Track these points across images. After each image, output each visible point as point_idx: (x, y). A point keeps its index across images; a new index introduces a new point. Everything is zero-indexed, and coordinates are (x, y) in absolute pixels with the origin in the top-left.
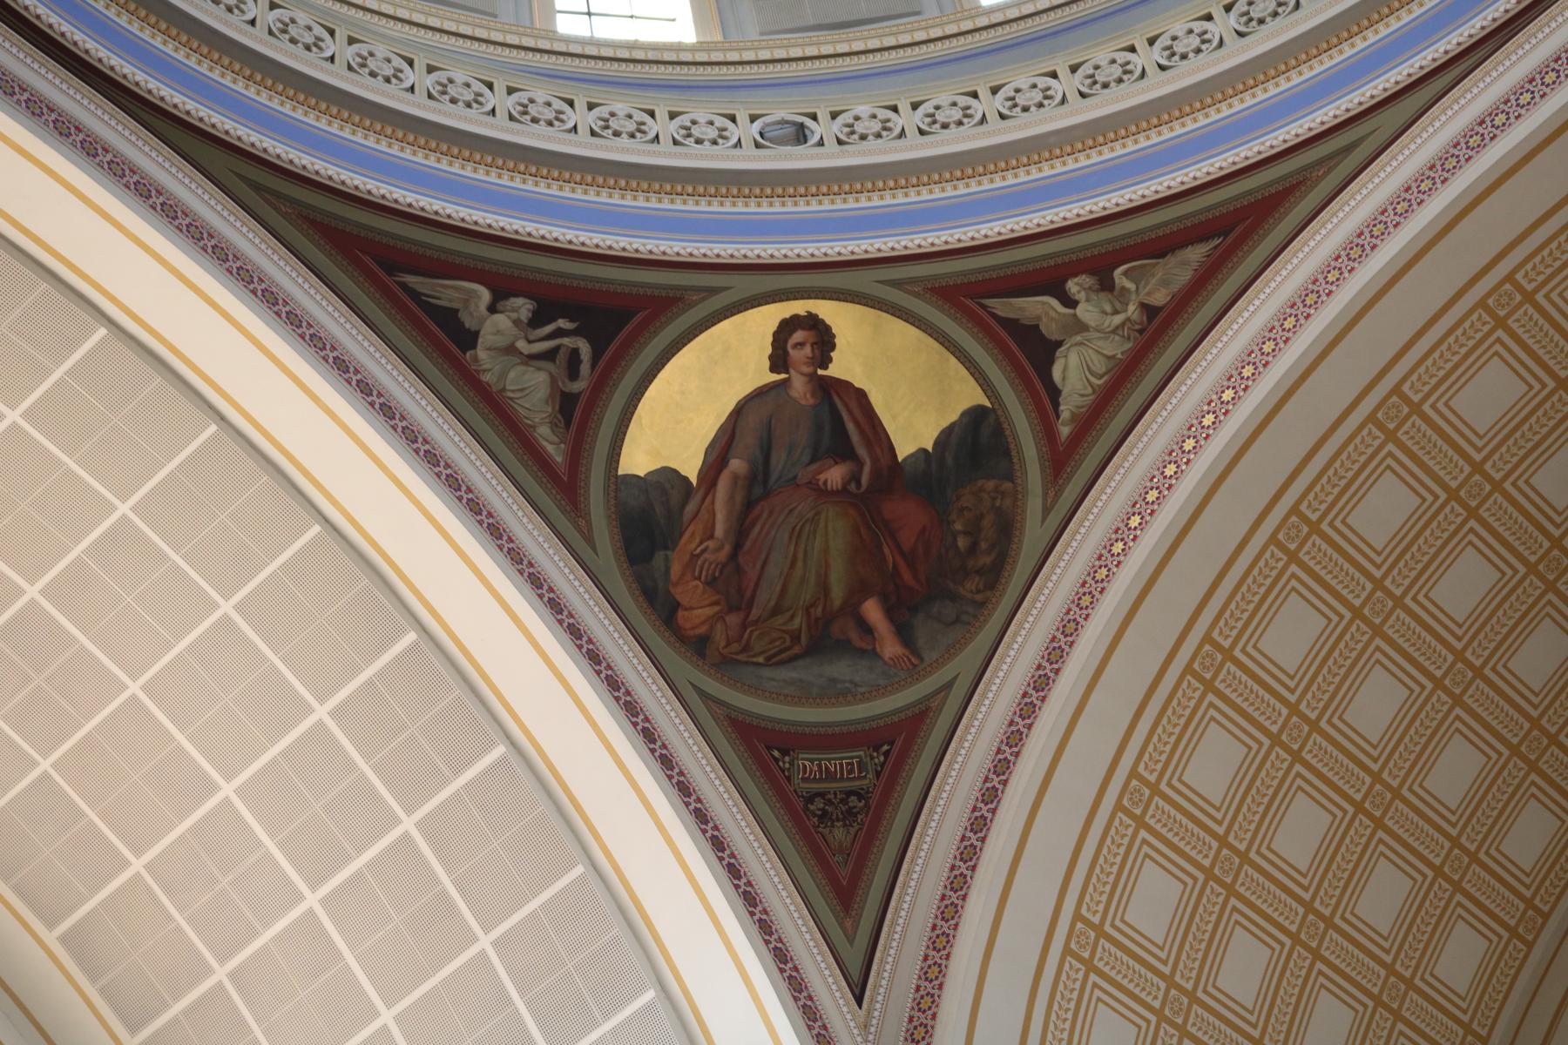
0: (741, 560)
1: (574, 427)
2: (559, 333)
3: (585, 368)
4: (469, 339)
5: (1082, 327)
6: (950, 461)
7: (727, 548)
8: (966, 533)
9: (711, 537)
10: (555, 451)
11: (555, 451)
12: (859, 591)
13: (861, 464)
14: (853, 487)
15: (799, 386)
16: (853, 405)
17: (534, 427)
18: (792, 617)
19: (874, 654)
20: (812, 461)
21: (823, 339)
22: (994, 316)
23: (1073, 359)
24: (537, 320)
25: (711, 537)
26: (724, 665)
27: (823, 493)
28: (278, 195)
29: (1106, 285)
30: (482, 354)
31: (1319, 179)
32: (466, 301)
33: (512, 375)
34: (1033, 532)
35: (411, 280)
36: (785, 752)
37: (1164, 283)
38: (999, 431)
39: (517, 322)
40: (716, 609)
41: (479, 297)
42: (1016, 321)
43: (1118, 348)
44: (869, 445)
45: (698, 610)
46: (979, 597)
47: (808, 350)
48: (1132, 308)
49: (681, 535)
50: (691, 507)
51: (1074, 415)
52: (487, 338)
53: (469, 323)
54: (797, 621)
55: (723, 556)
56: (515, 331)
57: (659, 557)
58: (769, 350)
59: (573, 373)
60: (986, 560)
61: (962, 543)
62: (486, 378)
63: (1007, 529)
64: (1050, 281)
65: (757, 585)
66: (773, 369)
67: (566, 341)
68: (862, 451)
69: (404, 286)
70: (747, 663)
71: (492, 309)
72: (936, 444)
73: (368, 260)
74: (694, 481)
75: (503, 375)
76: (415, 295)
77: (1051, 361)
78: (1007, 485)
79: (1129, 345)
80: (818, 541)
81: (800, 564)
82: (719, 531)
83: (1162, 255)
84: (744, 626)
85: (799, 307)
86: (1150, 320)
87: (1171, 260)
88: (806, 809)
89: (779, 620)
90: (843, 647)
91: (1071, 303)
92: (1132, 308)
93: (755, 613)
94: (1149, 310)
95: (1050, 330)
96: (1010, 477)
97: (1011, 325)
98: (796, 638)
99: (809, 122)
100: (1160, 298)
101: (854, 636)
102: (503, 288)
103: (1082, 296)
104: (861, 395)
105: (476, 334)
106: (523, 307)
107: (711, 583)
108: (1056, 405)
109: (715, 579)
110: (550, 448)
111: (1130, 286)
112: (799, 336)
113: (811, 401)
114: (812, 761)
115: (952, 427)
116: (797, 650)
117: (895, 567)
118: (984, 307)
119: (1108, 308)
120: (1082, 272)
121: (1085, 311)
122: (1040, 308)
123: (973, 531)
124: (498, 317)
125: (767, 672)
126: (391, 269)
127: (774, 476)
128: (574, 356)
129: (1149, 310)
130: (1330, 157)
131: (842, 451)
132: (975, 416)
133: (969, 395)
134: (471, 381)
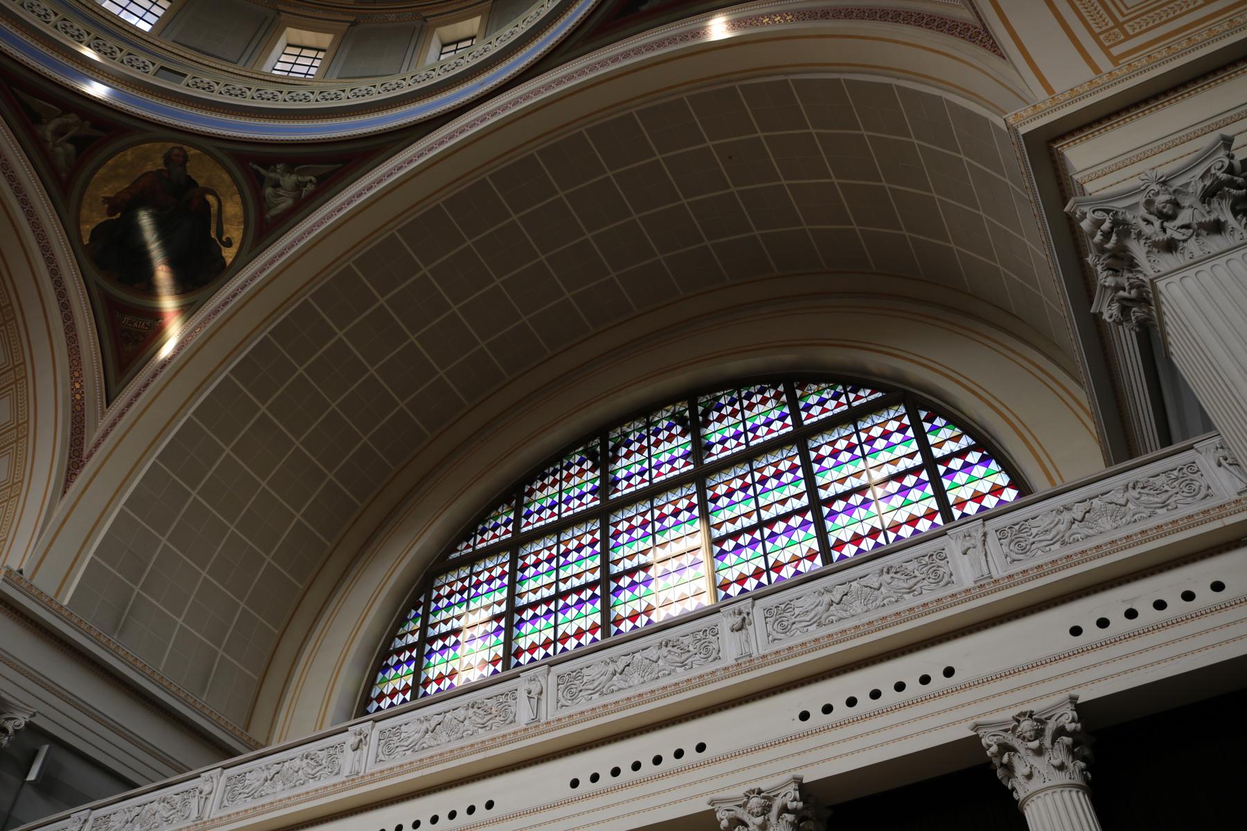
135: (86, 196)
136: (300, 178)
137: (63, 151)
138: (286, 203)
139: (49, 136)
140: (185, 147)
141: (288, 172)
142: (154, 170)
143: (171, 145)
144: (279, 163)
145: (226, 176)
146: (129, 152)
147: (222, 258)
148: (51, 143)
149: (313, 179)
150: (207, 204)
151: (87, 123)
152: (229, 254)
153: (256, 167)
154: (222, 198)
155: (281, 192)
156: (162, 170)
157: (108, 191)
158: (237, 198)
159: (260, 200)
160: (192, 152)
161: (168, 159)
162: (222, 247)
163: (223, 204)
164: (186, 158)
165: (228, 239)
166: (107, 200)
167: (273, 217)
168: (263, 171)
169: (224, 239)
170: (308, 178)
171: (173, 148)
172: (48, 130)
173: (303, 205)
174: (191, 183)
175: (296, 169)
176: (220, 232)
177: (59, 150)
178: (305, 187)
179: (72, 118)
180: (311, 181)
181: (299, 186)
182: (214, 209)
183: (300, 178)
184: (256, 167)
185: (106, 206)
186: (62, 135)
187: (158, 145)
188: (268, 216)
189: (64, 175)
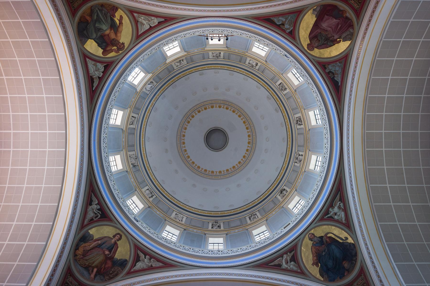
0: (89, 251)
1: (90, 222)
2: (99, 213)
3: (97, 218)
4: (91, 204)
5: (144, 261)
6: (119, 262)
7: (89, 249)
8: (112, 271)
9: (89, 246)
10: (86, 222)
11: (86, 222)
12: (96, 267)
13: (110, 254)
14: (107, 255)
15: (113, 241)
16: (116, 247)
17: (86, 218)
18: (87, 262)
19: (90, 275)
20: (106, 249)
21: (120, 239)
22: (137, 252)
23: (140, 264)
24: (98, 210)
25: (89, 246)
26: (75, 260)
27: (104, 253)
28: (91, 175)
29: (150, 259)
30: (90, 207)
31: (178, 267)
32: (95, 201)
33: (90, 212)
34: (119, 277)
35: (93, 194)
36: (70, 275)
37: (155, 264)
38: (126, 264)
39: (96, 208)
40: (81, 254)
41: (96, 202)
42: (139, 255)
43: (145, 267)
44: (113, 253)
45: (80, 252)
46: (107, 279)
47: (118, 238)
48: (150, 264)
49: (87, 243)
50: (91, 241)
51: (134, 270)
52: (92, 206)
53: (92, 203)
54: (87, 263)
55: (88, 249)
56: (95, 208)
57: (83, 243)
58: (114, 234)
59: (96, 218)
60: (111, 276)
61: (111, 272)
62: (88, 210)
63: (117, 275)
64: (145, 254)
65: (88, 255)
66: (113, 236)
67: (99, 214)
68: (112, 253)
69: (91, 194)
70: (77, 262)
71: (96, 204)
72: (119, 259)
73: (91, 189)
74: (94, 239)
75: (90, 211)
76: (91, 196)
77: (138, 262)
78: (121, 270)
79: (146, 267)
80: (98, 257)
81: (94, 258)
82: (91, 246)
83: (158, 261)
84: (82, 258)
85: (121, 233)
86: (151, 267)
87: (158, 263)
88: (65, 284)
89: (86, 261)
90: (88, 271)
91: (145, 258)
92: (150, 264)
93: (84, 258)
94: (151, 265)
95: (141, 259)
96: (122, 270)
97: (138, 255)
98: (85, 265)
99: (139, 221)
100: (154, 266)
101: (91, 271)
102: (99, 204)
103: (147, 258)
104: (118, 247)
105: (92, 205)
106: (99, 207)
107: (84, 251)
108: (134, 267)
109: (85, 250)
110: (85, 222)
111: (152, 262)
112: (119, 236)
113: (113, 243)
114: (71, 279)
115: (123, 259)
116: (84, 266)
117: (102, 268)
118: (137, 250)
119: (148, 262)
120: (149, 256)
121: (146, 260)
122: (142, 256)
123: (113, 272)
124: (95, 206)
125: (78, 265)
126: (92, 192)
127: (101, 247)
128: (97, 216)
129: (151, 265)
130: (181, 266)
131: (110, 251)
132: (126, 261)
133: (127, 258)
134: (87, 208)
135: (308, 269)
136: (337, 206)
137: (292, 266)
138: (343, 214)
139: (286, 266)
140: (310, 232)
141: (333, 208)
142: (312, 245)
143: (307, 236)
144: (329, 209)
145: (325, 227)
146: (303, 248)
147: (350, 243)
148: (288, 267)
149: (340, 202)
150: (330, 237)
151: (288, 253)
152: (350, 240)
153: (327, 217)
154: (330, 232)
155: (338, 214)
156: (313, 243)
157: (311, 262)
158: (333, 227)
159: (337, 221)
160: (312, 231)
161: (311, 239)
162: (347, 241)
163: (332, 232)
164: (313, 234)
165: (345, 238)
166: (313, 264)
167: (345, 221)
168: (329, 215)
169: (344, 239)
170: (338, 204)
171: (308, 236)
172: (284, 265)
173: (346, 209)
174: (321, 237)
175: (333, 205)
176: (341, 239)
177: (291, 266)
178: (340, 206)
179: (285, 256)
180: (340, 203)
181: (339, 208)
182: (333, 236)
183: (337, 206)
184: (327, 217)
185: (315, 266)
186: (288, 263)
187: (305, 239)
188: (344, 222)
189: (299, 271)
